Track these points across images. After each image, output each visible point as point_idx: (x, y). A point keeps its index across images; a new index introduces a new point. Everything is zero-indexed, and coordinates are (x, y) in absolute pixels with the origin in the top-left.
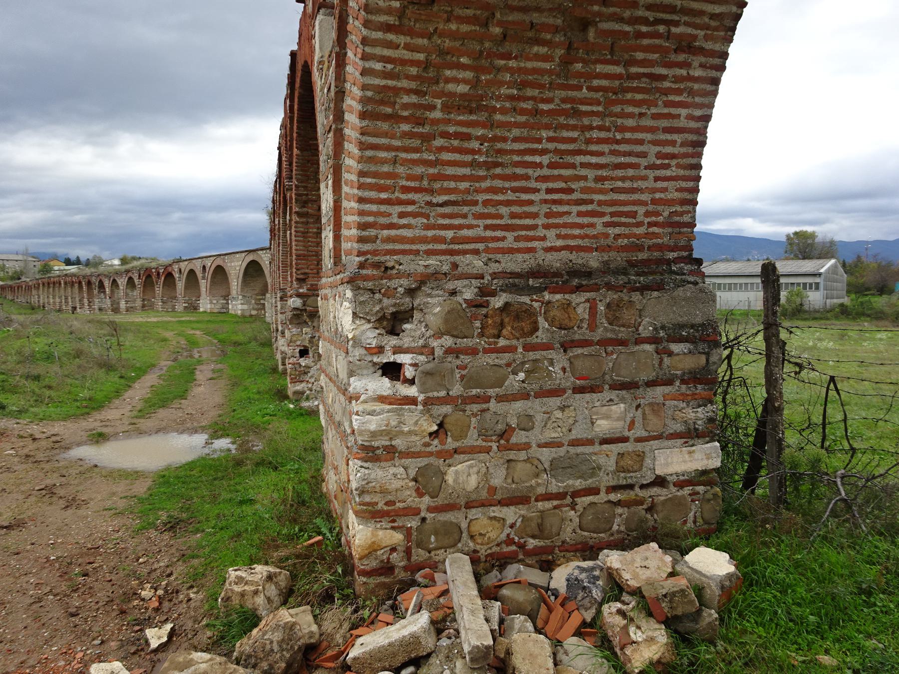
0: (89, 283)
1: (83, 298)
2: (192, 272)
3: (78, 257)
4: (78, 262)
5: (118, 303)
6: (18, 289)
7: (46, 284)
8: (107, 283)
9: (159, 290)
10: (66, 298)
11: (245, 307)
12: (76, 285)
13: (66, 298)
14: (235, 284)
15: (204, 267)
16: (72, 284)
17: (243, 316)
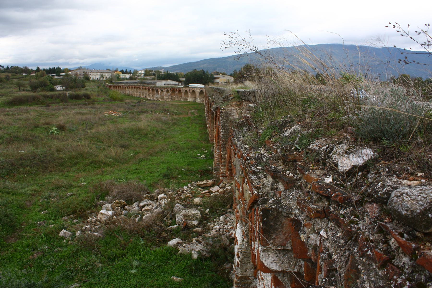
0: (153, 90)
1: (150, 94)
2: (186, 91)
3: (126, 70)
4: (126, 72)
5: (163, 97)
6: (118, 87)
7: (133, 88)
8: (159, 91)
9: (176, 94)
10: (143, 93)
11: (199, 101)
12: (147, 90)
13: (143, 93)
14: (197, 95)
15: (190, 90)
16: (146, 89)
17: (199, 103)
